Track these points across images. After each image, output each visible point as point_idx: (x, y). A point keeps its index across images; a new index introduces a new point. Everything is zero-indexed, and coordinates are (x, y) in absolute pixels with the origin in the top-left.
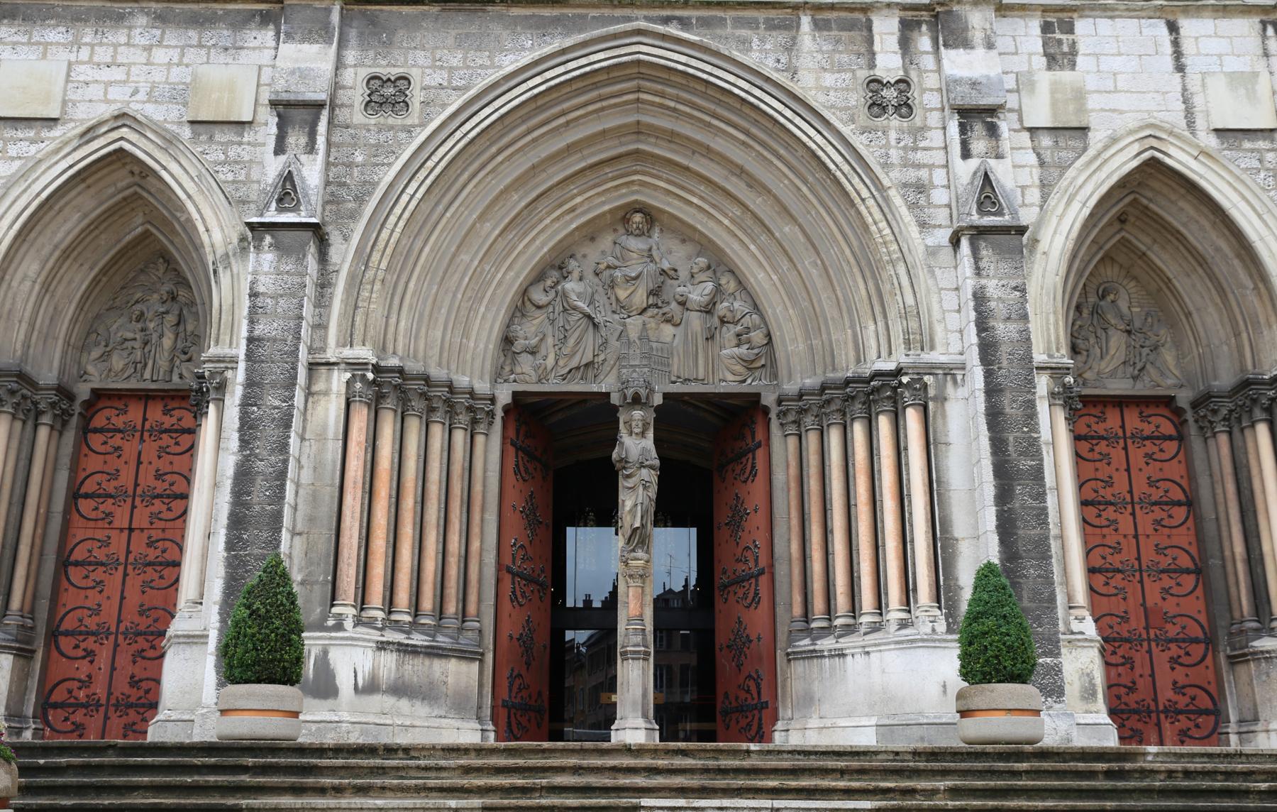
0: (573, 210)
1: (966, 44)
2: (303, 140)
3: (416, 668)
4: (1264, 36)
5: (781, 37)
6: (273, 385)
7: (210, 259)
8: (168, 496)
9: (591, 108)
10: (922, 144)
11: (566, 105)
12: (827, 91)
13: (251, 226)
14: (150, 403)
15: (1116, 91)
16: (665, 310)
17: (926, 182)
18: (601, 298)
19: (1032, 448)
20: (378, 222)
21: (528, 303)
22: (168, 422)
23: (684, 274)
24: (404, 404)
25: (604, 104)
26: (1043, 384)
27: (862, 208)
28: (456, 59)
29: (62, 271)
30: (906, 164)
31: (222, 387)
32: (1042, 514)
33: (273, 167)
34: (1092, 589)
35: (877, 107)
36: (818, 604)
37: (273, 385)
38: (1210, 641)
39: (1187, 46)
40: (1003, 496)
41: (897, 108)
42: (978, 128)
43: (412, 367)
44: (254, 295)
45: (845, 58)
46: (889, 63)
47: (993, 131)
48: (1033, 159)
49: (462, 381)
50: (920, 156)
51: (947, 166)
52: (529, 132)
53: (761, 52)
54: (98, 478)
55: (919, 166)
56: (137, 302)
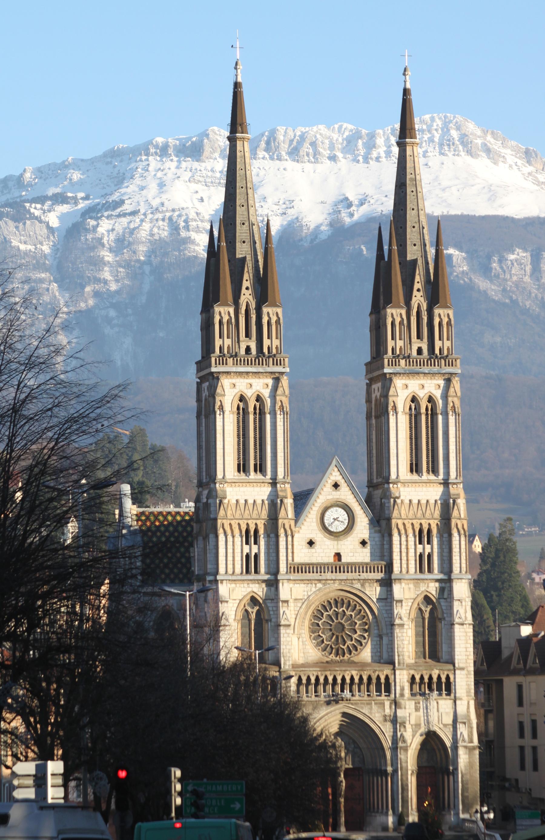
5: (369, 706)
42: (402, 727)
45: (380, 710)
47: (405, 727)
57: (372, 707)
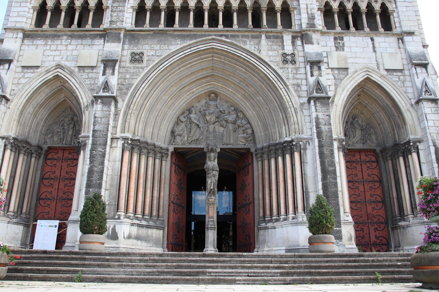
0: (193, 92)
1: (312, 43)
2: (111, 71)
3: (143, 232)
4: (399, 43)
5: (256, 41)
6: (100, 144)
7: (82, 107)
8: (70, 179)
9: (198, 62)
10: (299, 72)
11: (191, 61)
12: (270, 57)
13: (95, 97)
14: (65, 151)
15: (356, 57)
16: (221, 123)
17: (300, 84)
18: (201, 120)
19: (333, 164)
20: (133, 96)
21: (179, 121)
22: (70, 156)
23: (227, 112)
24: (140, 151)
25: (202, 60)
26: (336, 144)
27: (281, 91)
28: (157, 47)
29: (40, 111)
30: (294, 78)
31: (85, 145)
32: (336, 184)
33: (102, 79)
34: (351, 208)
35: (285, 61)
36: (268, 212)
37: (100, 144)
38: (387, 223)
39: (376, 45)
40: (324, 178)
41: (291, 62)
42: (315, 68)
43: (142, 139)
44: (95, 117)
45: (275, 47)
46: (288, 49)
47: (319, 68)
48: (332, 77)
49: (158, 144)
50: (298, 76)
51: (306, 79)
52: (179, 69)
53: (250, 46)
54: (49, 173)
55: (298, 79)
56: (62, 121)
57: (260, 42)
